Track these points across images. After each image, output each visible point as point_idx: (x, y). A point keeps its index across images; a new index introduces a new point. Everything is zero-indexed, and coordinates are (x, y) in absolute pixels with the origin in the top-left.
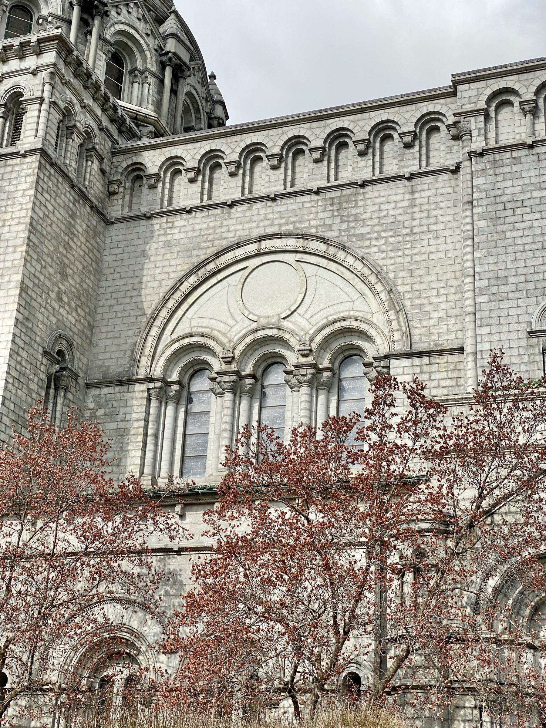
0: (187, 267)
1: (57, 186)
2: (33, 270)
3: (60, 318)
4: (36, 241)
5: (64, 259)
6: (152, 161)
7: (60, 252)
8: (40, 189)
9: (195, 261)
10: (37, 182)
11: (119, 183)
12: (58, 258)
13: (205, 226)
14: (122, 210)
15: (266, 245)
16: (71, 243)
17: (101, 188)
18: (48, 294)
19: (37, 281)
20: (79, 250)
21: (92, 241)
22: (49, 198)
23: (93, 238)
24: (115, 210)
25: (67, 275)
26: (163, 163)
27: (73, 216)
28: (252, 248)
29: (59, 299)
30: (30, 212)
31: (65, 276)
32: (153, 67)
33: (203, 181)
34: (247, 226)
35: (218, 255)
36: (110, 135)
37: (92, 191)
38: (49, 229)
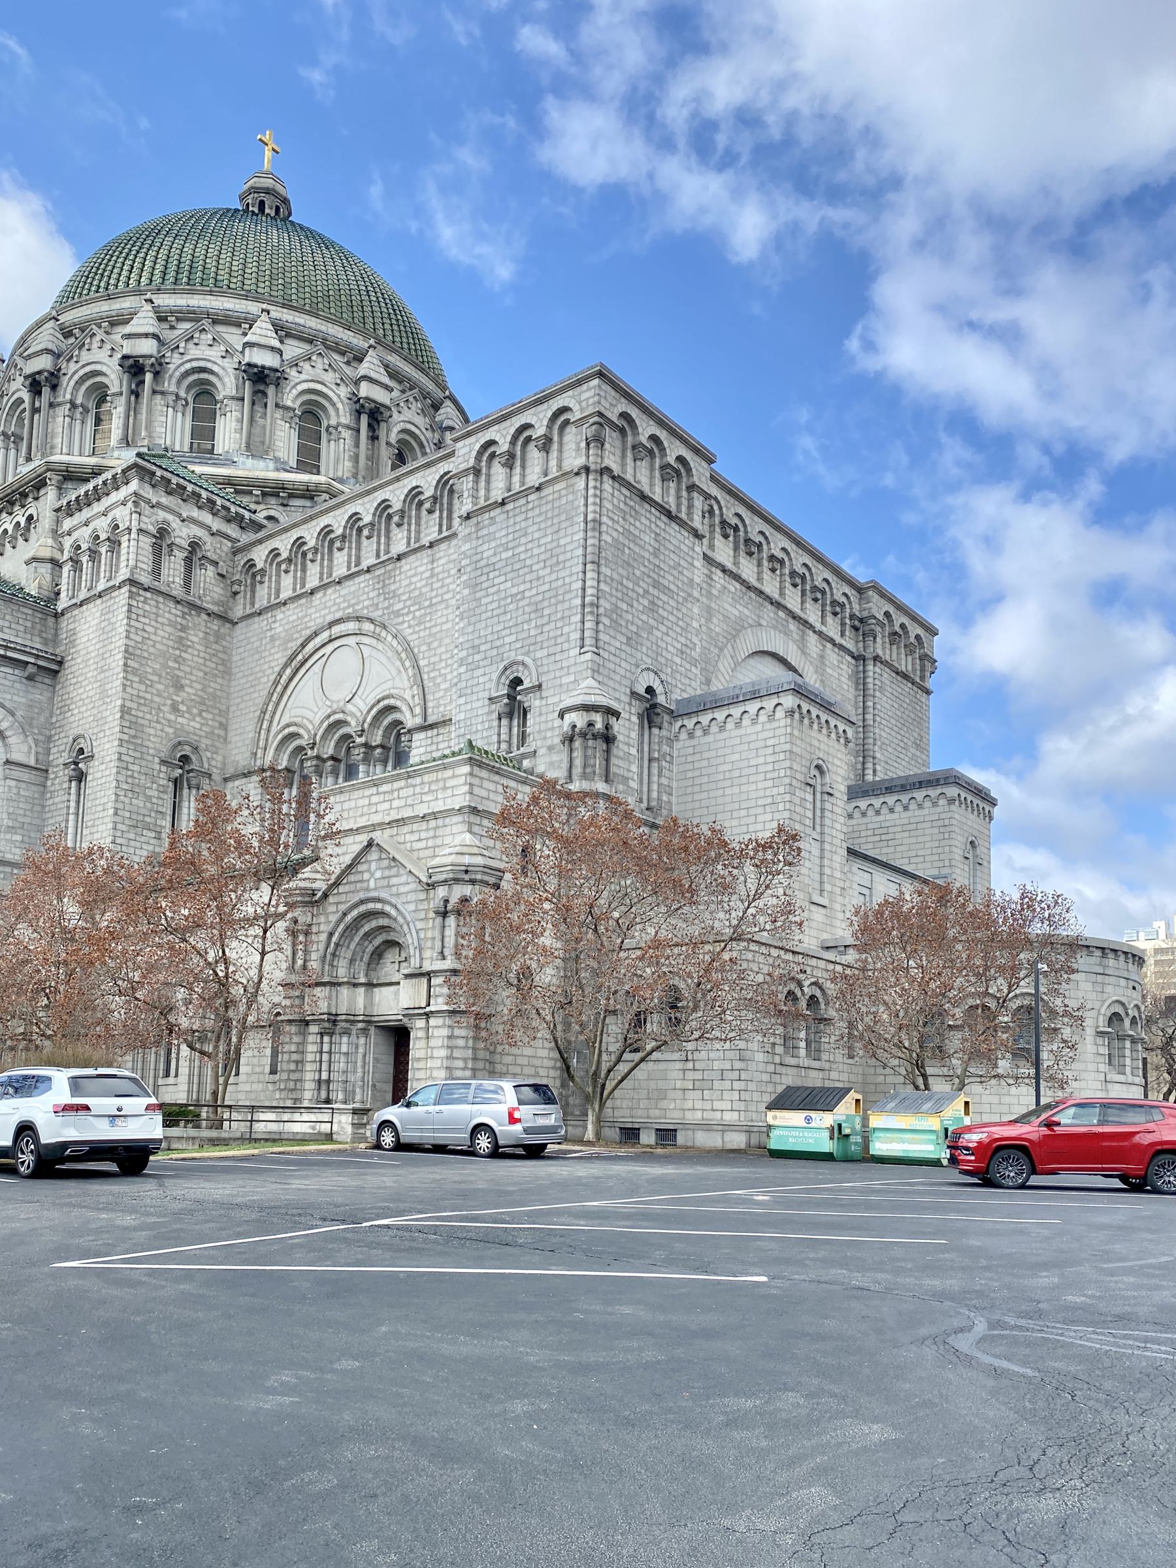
0: (283, 661)
1: (157, 607)
2: (135, 692)
3: (179, 726)
4: (136, 665)
5: (177, 672)
6: (259, 555)
7: (169, 667)
8: (134, 616)
9: (290, 652)
10: (129, 611)
11: (239, 583)
12: (167, 673)
13: (295, 617)
14: (245, 608)
15: (337, 630)
16: (183, 655)
17: (221, 592)
18: (159, 708)
19: (142, 701)
20: (196, 659)
21: (214, 646)
22: (147, 621)
23: (216, 643)
24: (238, 611)
25: (182, 687)
26: (268, 556)
27: (184, 629)
28: (325, 636)
29: (175, 709)
30: (124, 641)
31: (179, 687)
32: (346, 419)
33: (296, 571)
34: (323, 613)
35: (303, 645)
36: (227, 537)
37: (208, 598)
38: (152, 650)
